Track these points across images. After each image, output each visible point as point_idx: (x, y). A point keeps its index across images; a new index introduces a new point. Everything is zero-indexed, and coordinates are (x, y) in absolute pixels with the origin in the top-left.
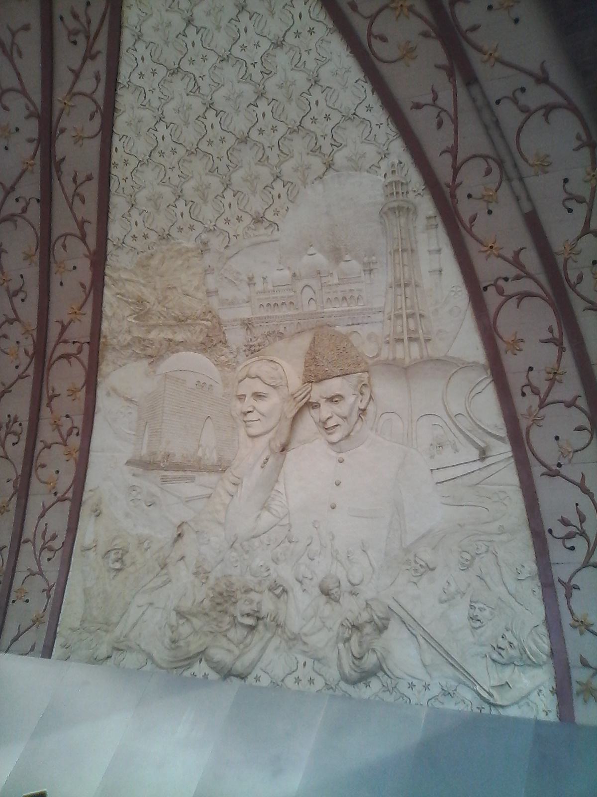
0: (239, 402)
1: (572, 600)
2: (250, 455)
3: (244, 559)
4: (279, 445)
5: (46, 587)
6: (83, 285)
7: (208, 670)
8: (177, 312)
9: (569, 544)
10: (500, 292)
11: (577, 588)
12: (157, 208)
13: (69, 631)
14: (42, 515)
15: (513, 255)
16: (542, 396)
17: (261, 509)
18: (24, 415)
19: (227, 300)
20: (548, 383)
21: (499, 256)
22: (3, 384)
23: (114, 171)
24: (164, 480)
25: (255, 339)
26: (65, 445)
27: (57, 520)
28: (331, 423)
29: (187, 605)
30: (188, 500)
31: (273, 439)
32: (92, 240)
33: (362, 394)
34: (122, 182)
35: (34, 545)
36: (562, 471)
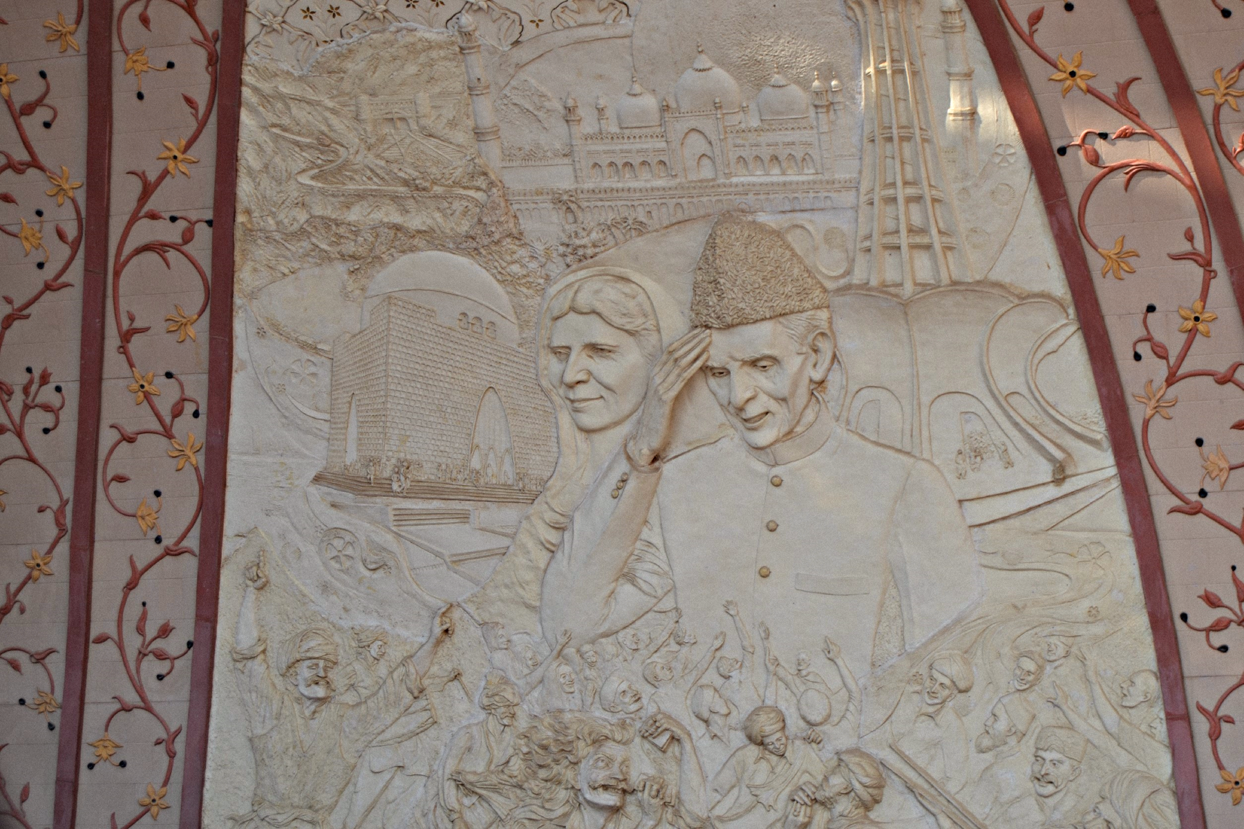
0: (553, 360)
1: (1219, 742)
2: (583, 465)
3: (586, 679)
4: (645, 451)
5: (164, 736)
6: (189, 101)
8: (410, 171)
9: (1218, 639)
11: (1230, 720)
13: (230, 824)
14: (131, 585)
15: (1114, 89)
16: (1172, 361)
17: (617, 580)
18: (67, 372)
19: (520, 149)
20: (1185, 336)
21: (1090, 91)
22: (9, 301)
24: (402, 517)
25: (584, 234)
26: (169, 435)
29: (476, 766)
30: (458, 560)
31: (633, 437)
33: (816, 351)
35: (121, 647)
36: (1207, 503)
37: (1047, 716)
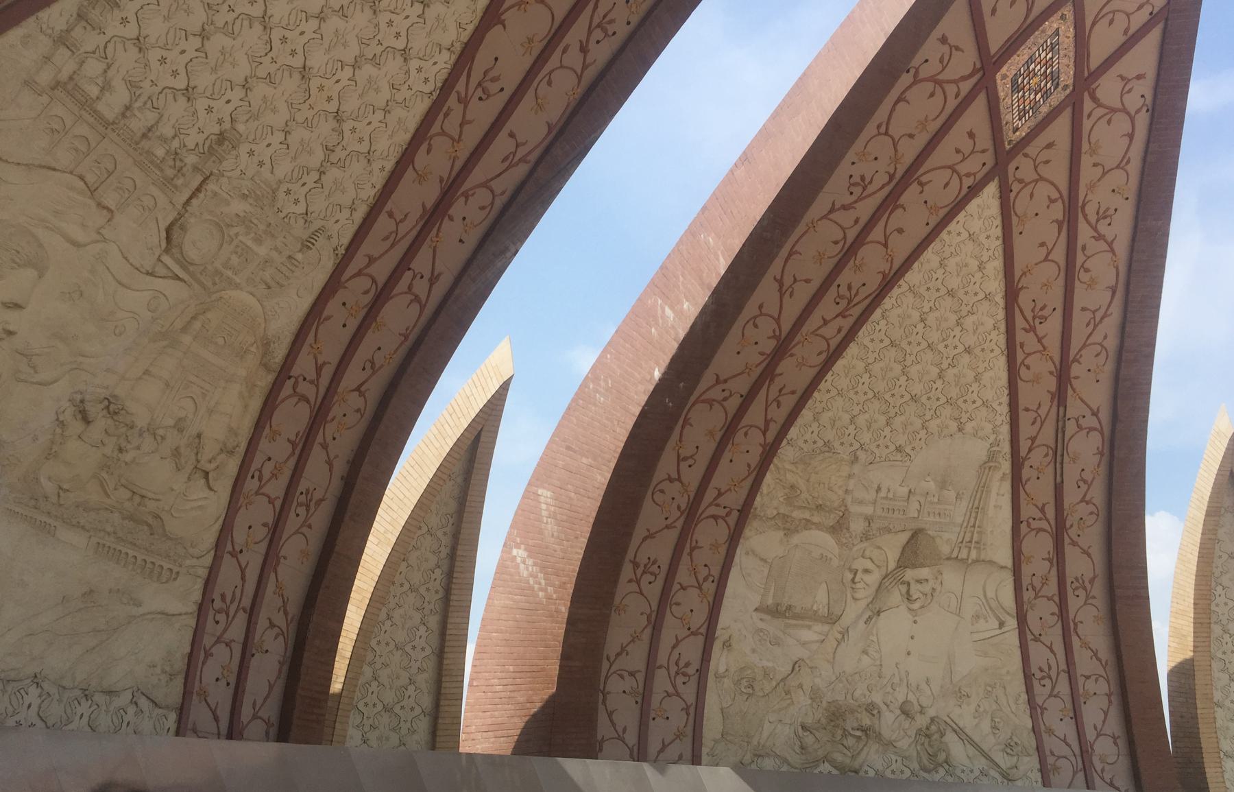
6: (749, 466)
7: (831, 769)
10: (1029, 525)
12: (833, 426)
14: (674, 647)
18: (664, 562)
23: (816, 394)
26: (700, 587)
27: (691, 651)
28: (915, 597)
29: (809, 721)
30: (804, 644)
32: (770, 436)
34: (818, 404)
35: (668, 669)
37: (994, 707)
